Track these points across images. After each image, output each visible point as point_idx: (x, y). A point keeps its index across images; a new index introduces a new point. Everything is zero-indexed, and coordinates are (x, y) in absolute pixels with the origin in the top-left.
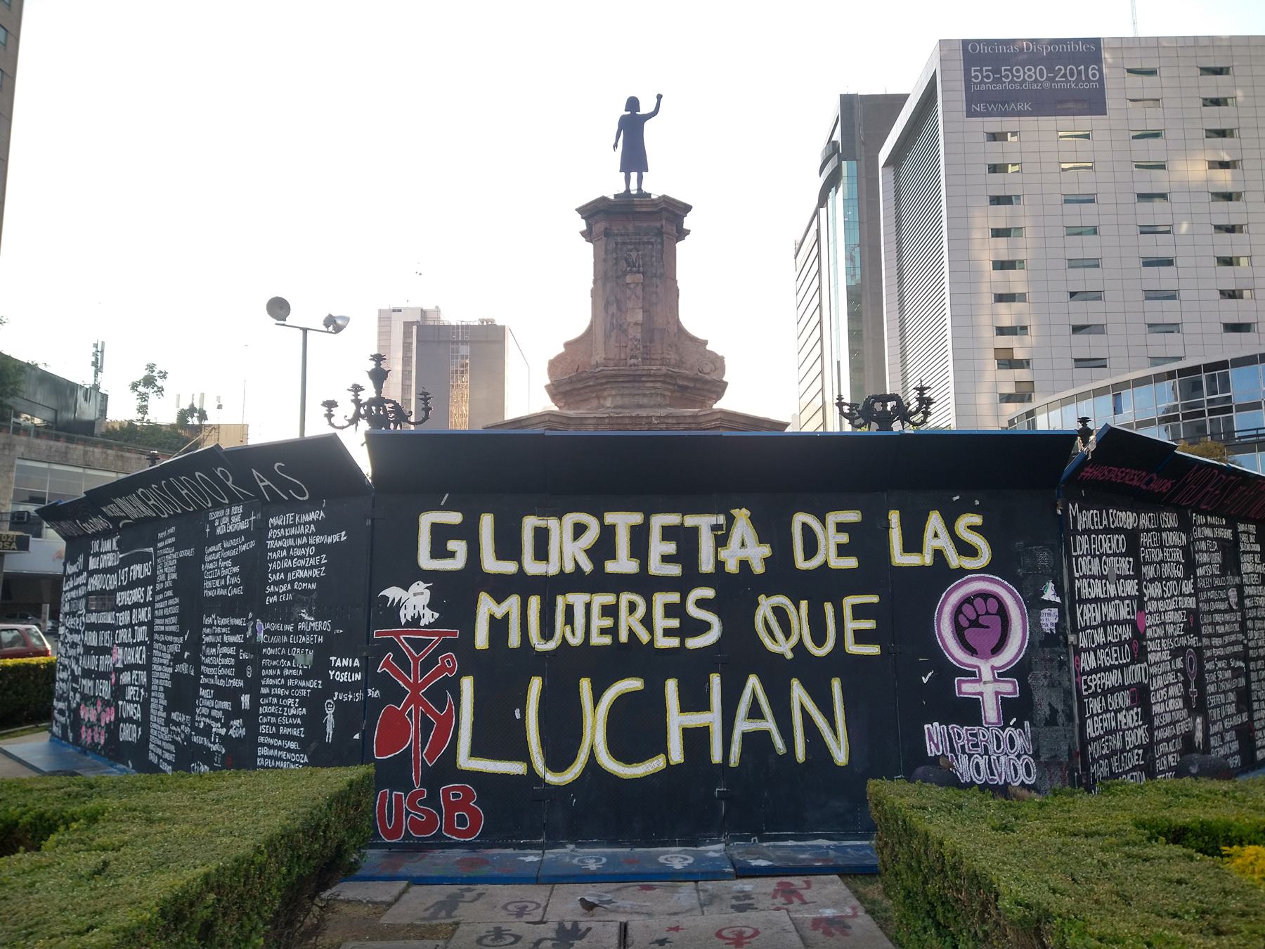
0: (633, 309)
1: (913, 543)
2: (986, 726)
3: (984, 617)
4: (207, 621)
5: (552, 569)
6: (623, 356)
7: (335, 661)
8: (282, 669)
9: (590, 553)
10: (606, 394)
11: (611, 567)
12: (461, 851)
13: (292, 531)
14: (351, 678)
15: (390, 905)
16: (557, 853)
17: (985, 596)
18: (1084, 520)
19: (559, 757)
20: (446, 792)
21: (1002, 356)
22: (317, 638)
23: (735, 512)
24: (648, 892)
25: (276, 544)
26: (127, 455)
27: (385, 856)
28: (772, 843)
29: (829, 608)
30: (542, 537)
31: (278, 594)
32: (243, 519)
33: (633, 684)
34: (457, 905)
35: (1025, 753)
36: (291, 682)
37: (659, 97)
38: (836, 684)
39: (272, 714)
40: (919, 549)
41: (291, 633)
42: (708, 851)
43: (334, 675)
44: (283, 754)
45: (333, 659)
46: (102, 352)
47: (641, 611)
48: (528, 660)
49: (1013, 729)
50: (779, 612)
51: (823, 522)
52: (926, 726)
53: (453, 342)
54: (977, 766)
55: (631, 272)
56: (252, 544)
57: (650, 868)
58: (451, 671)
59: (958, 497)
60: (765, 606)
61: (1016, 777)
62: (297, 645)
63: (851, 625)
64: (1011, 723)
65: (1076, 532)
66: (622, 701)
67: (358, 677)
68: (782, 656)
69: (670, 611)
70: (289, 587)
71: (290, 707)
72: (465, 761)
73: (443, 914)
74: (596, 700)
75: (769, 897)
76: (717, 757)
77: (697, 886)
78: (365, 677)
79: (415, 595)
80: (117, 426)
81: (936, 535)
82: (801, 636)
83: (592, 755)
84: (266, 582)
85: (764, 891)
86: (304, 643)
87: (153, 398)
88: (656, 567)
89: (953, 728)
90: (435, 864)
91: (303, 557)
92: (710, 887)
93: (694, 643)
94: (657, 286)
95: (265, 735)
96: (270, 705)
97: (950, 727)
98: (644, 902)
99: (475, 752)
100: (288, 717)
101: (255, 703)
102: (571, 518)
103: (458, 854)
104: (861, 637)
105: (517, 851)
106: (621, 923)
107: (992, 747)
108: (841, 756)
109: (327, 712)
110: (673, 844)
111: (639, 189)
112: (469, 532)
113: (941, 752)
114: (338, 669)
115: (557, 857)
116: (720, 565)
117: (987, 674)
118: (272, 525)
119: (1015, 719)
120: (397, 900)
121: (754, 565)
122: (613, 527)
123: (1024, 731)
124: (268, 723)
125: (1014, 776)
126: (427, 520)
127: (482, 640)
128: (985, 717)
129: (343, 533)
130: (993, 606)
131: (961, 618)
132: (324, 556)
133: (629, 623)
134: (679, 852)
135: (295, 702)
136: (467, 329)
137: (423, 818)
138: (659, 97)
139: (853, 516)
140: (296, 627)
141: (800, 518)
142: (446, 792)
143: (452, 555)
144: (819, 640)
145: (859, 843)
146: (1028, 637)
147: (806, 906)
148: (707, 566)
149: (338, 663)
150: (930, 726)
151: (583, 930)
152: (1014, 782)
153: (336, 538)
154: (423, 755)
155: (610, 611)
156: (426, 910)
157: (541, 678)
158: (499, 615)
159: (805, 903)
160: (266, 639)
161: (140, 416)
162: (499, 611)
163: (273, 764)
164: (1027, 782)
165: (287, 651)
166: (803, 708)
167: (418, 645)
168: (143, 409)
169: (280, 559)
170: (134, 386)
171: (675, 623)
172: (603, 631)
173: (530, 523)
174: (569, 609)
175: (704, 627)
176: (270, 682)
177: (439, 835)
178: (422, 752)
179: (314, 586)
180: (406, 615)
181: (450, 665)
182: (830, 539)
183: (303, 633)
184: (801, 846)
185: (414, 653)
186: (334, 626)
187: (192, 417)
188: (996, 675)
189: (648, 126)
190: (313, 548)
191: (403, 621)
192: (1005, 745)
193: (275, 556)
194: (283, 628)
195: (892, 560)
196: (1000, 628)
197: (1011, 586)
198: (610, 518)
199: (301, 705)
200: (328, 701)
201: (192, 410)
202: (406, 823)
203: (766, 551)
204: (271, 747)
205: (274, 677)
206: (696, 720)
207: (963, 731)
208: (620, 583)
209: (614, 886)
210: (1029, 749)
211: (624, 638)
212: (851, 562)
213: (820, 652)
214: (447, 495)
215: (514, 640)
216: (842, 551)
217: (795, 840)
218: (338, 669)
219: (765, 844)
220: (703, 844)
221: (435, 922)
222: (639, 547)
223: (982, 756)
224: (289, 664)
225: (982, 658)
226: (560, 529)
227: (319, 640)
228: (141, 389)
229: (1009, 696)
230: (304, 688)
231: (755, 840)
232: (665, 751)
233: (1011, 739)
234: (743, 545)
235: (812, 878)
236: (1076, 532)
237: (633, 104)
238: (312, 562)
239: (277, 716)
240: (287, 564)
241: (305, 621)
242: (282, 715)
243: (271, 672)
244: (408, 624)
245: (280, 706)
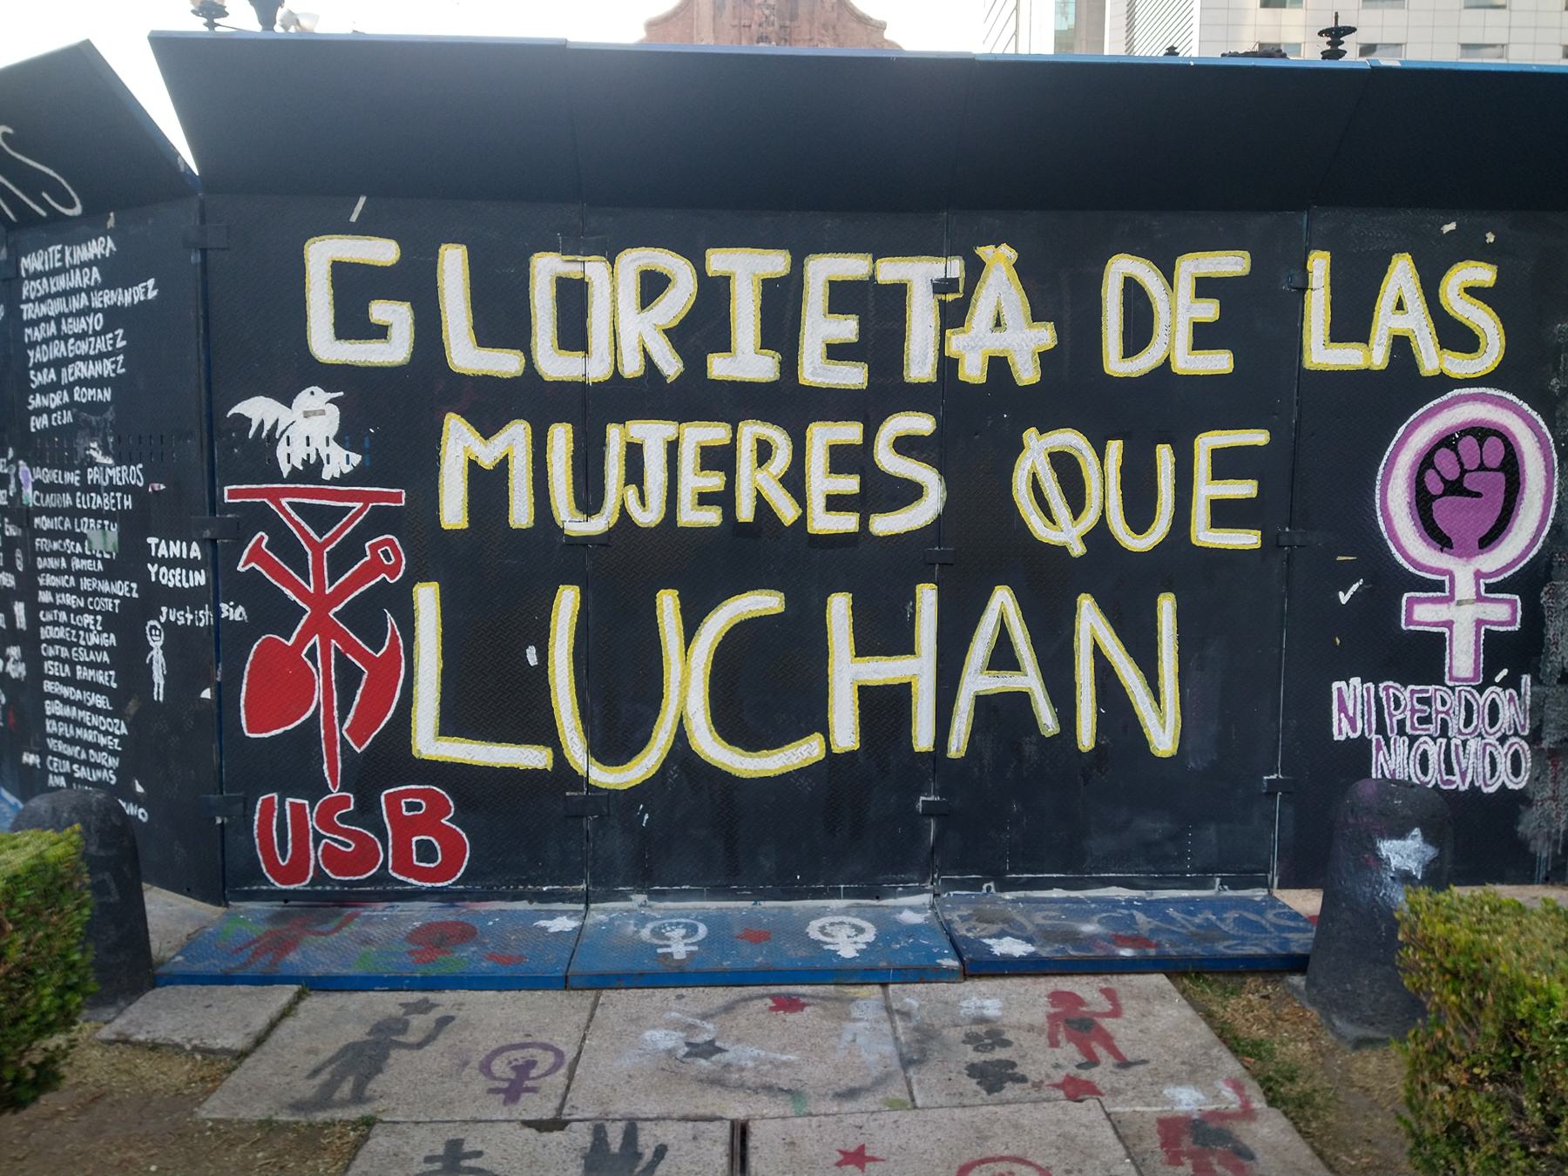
2: (1451, 684)
3: (1475, 474)
5: (596, 368)
7: (157, 546)
8: (69, 558)
9: (677, 336)
11: (719, 367)
12: (426, 905)
14: (188, 581)
15: (242, 1055)
16: (614, 910)
17: (1481, 432)
20: (393, 801)
22: (122, 498)
23: (985, 252)
24: (791, 1017)
25: (37, 310)
27: (276, 918)
28: (1021, 894)
30: (573, 297)
31: (47, 410)
33: (765, 602)
34: (386, 1057)
35: (1516, 734)
36: (86, 584)
38: (1167, 606)
39: (62, 642)
41: (78, 489)
42: (900, 909)
43: (157, 574)
44: (84, 715)
45: (152, 541)
47: (782, 459)
49: (1499, 690)
50: (1065, 465)
51: (1168, 273)
52: (1336, 685)
54: (1424, 758)
57: (795, 955)
58: (393, 571)
59: (1452, 226)
61: (1492, 776)
62: (90, 513)
63: (1207, 489)
64: (1498, 679)
66: (741, 635)
67: (199, 578)
68: (1063, 550)
69: (841, 459)
70: (66, 399)
71: (88, 630)
72: (428, 742)
73: (346, 1089)
74: (690, 630)
75: (1044, 1040)
76: (923, 738)
77: (886, 996)
78: (214, 577)
79: (307, 415)
81: (1400, 306)
82: (1104, 511)
83: (681, 736)
84: (26, 389)
85: (1026, 1020)
86: (100, 509)
88: (815, 370)
89: (1386, 689)
90: (367, 941)
91: (82, 336)
92: (912, 1002)
93: (885, 524)
95: (53, 678)
96: (56, 623)
97: (1381, 686)
98: (783, 1050)
99: (450, 725)
100: (88, 648)
101: (34, 622)
102: (635, 260)
103: (418, 913)
104: (1224, 514)
105: (536, 906)
106: (733, 1123)
107: (1457, 722)
108: (1163, 736)
109: (152, 643)
110: (834, 894)
113: (1359, 733)
114: (163, 562)
115: (612, 920)
116: (947, 366)
117: (1465, 586)
118: (27, 270)
119: (1505, 672)
120: (259, 1041)
121: (1018, 366)
122: (726, 280)
123: (1519, 694)
124: (57, 658)
125: (1488, 775)
127: (453, 512)
128: (1451, 668)
129: (151, 282)
130: (1494, 452)
131: (1430, 475)
132: (120, 332)
134: (846, 911)
135: (96, 621)
137: (348, 846)
139: (1232, 264)
140: (83, 476)
141: (1121, 267)
142: (393, 801)
143: (381, 332)
144: (1139, 518)
145: (1185, 894)
146: (1551, 515)
147: (1130, 1075)
148: (920, 367)
149: (163, 551)
150: (1343, 684)
151: (648, 1154)
152: (1486, 785)
154: (343, 731)
155: (719, 459)
156: (315, 1072)
157: (577, 589)
158: (487, 462)
159: (1124, 1064)
160: (38, 499)
162: (488, 453)
163: (72, 732)
164: (1511, 786)
165: (73, 525)
166: (1097, 652)
167: (322, 519)
169: (46, 341)
171: (849, 484)
172: (705, 499)
173: (546, 269)
174: (634, 454)
175: (910, 492)
176: (52, 581)
177: (382, 877)
178: (341, 726)
179: (106, 395)
180: (290, 456)
181: (389, 559)
183: (96, 488)
184: (1077, 901)
185: (312, 533)
186: (149, 476)
188: (1483, 588)
190: (100, 315)
191: (285, 469)
192: (1481, 720)
193: (37, 335)
194: (63, 479)
195: (1306, 356)
196: (1501, 498)
197: (1534, 414)
198: (719, 261)
199: (107, 628)
200: (151, 623)
202: (314, 855)
203: (1045, 336)
204: (66, 701)
205: (57, 572)
206: (884, 670)
207: (1405, 694)
209: (719, 996)
210: (1523, 727)
211: (745, 512)
212: (1220, 362)
214: (362, 200)
215: (521, 514)
217: (1065, 888)
218: (163, 562)
219: (1008, 896)
220: (892, 894)
221: (321, 1116)
223: (1434, 740)
224: (79, 549)
225: (1460, 556)
227: (126, 503)
229: (1502, 629)
230: (108, 595)
231: (989, 889)
232: (826, 732)
233: (1494, 710)
234: (998, 323)
235: (1115, 982)
238: (102, 345)
239: (69, 645)
240: (57, 350)
241: (97, 464)
242: (78, 645)
243: (52, 563)
244: (295, 475)
245: (73, 627)
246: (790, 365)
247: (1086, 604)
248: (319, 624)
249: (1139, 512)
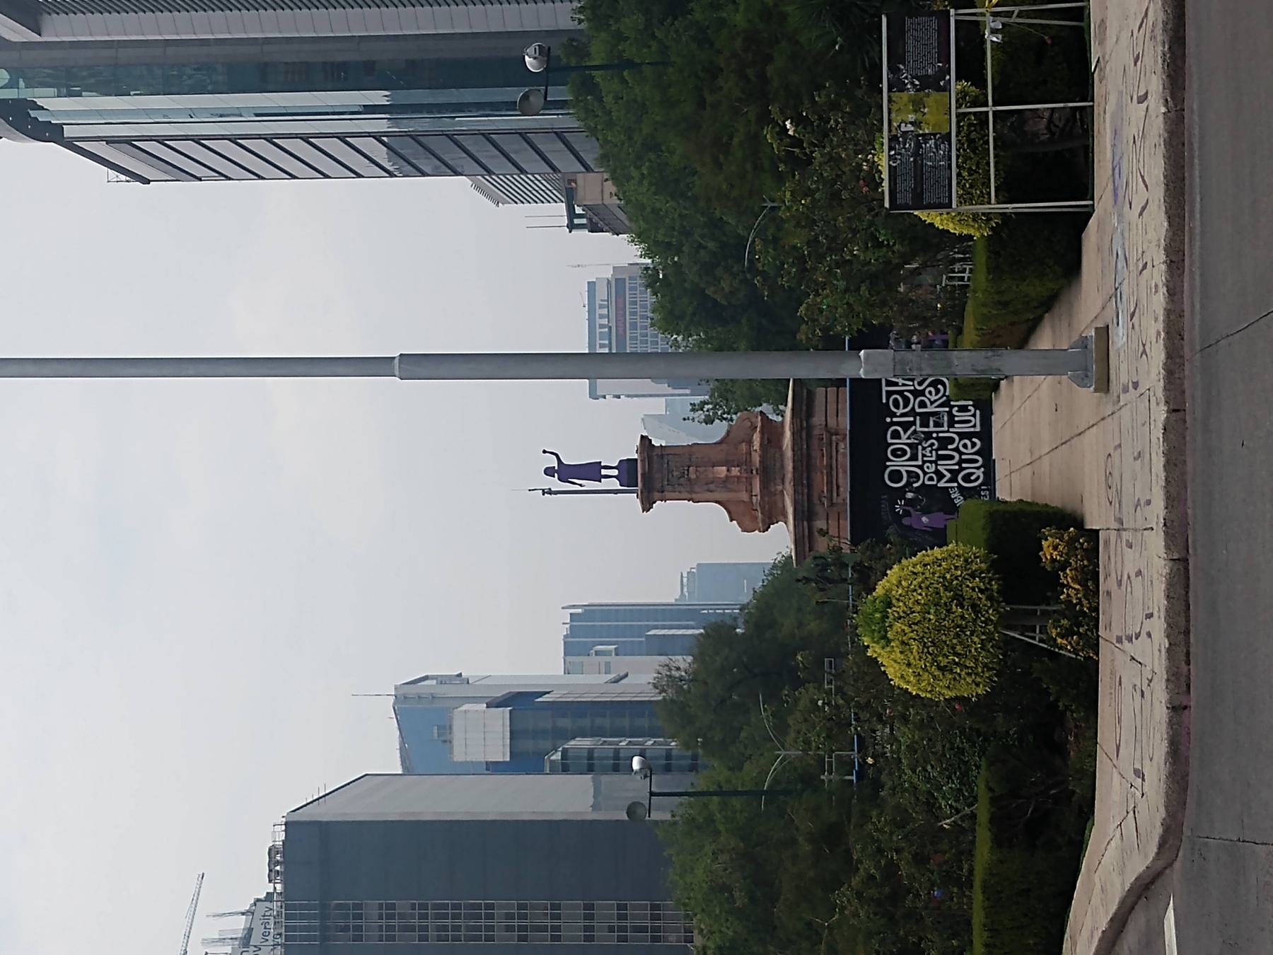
0: (713, 473)
6: (744, 480)
10: (773, 490)
55: (688, 475)
94: (697, 458)
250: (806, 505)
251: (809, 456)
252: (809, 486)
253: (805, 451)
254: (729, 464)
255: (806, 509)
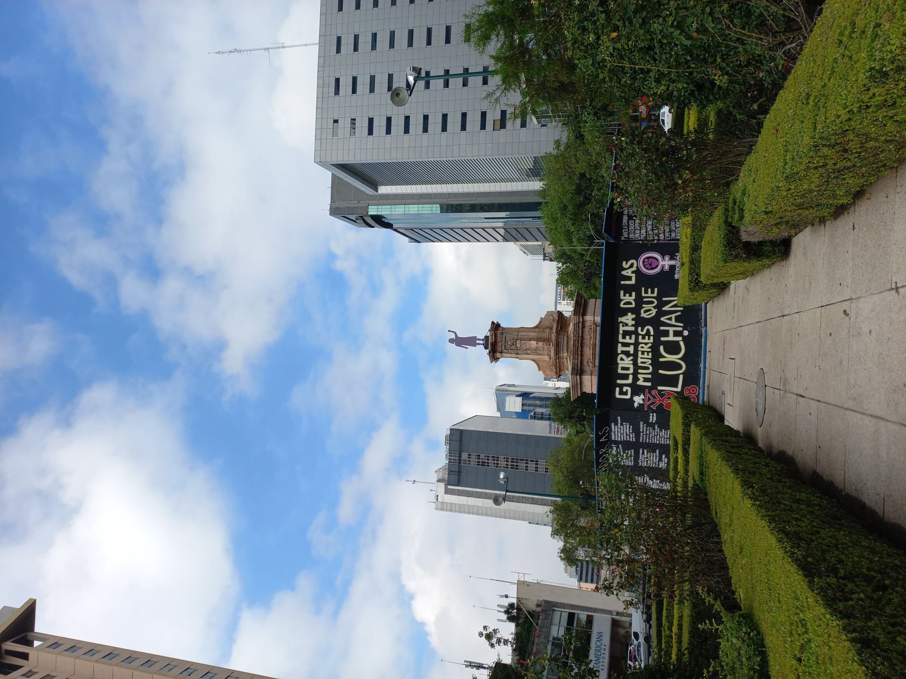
1: (629, 278)
4: (640, 464)
5: (631, 367)
11: (632, 352)
13: (616, 433)
17: (644, 262)
18: (625, 235)
19: (679, 367)
21: (498, 124)
26: (534, 650)
29: (645, 300)
30: (623, 369)
32: (613, 449)
33: (662, 348)
37: (449, 331)
38: (664, 299)
40: (631, 277)
46: (470, 662)
47: (643, 345)
48: (655, 373)
50: (645, 312)
53: (460, 463)
56: (620, 446)
60: (643, 315)
63: (649, 294)
65: (628, 238)
66: (665, 351)
69: (643, 338)
72: (679, 389)
74: (664, 357)
80: (518, 658)
83: (679, 359)
84: (629, 441)
87: (499, 636)
88: (632, 341)
93: (652, 333)
99: (676, 386)
102: (619, 361)
104: (652, 292)
111: (483, 340)
112: (621, 386)
116: (632, 325)
126: (618, 396)
127: (649, 384)
130: (646, 260)
133: (646, 348)
136: (451, 453)
138: (449, 331)
139: (622, 292)
141: (622, 305)
143: (627, 390)
144: (653, 302)
148: (633, 329)
153: (619, 420)
155: (643, 353)
161: (509, 643)
167: (649, 399)
168: (506, 642)
170: (492, 645)
171: (647, 337)
172: (648, 355)
173: (620, 371)
174: (642, 363)
175: (648, 330)
180: (641, 402)
182: (627, 298)
187: (512, 613)
189: (459, 336)
198: (619, 352)
201: (507, 612)
203: (629, 314)
206: (671, 333)
208: (636, 350)
211: (650, 350)
212: (634, 294)
213: (656, 302)
215: (649, 376)
216: (630, 295)
222: (627, 345)
226: (621, 364)
228: (494, 641)
236: (628, 238)
237: (451, 341)
240: (625, 435)
246: (632, 344)
247: (663, 309)
248: (662, 401)
249: (652, 302)
250: (579, 366)
251: (582, 337)
252: (582, 355)
253: (580, 335)
254: (538, 340)
255: (579, 369)
